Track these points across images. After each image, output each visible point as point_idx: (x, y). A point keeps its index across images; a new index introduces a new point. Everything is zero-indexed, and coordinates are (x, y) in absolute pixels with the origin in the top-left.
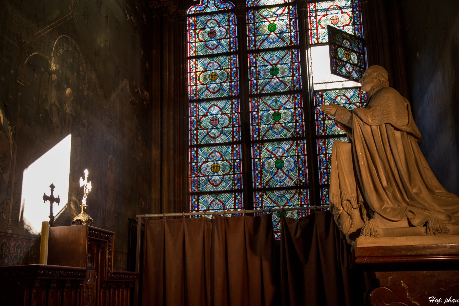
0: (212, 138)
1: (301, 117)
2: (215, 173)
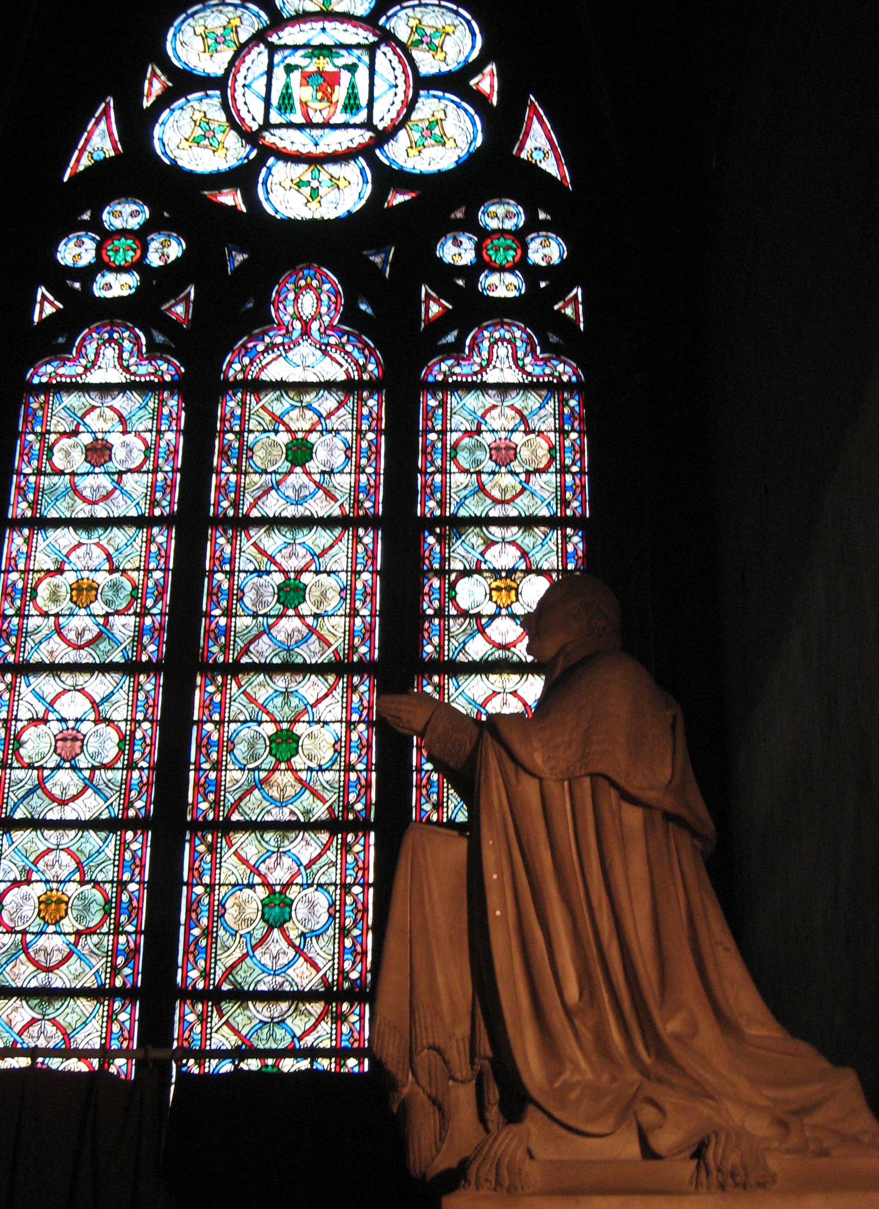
0: (54, 802)
1: (367, 753)
2: (49, 925)
